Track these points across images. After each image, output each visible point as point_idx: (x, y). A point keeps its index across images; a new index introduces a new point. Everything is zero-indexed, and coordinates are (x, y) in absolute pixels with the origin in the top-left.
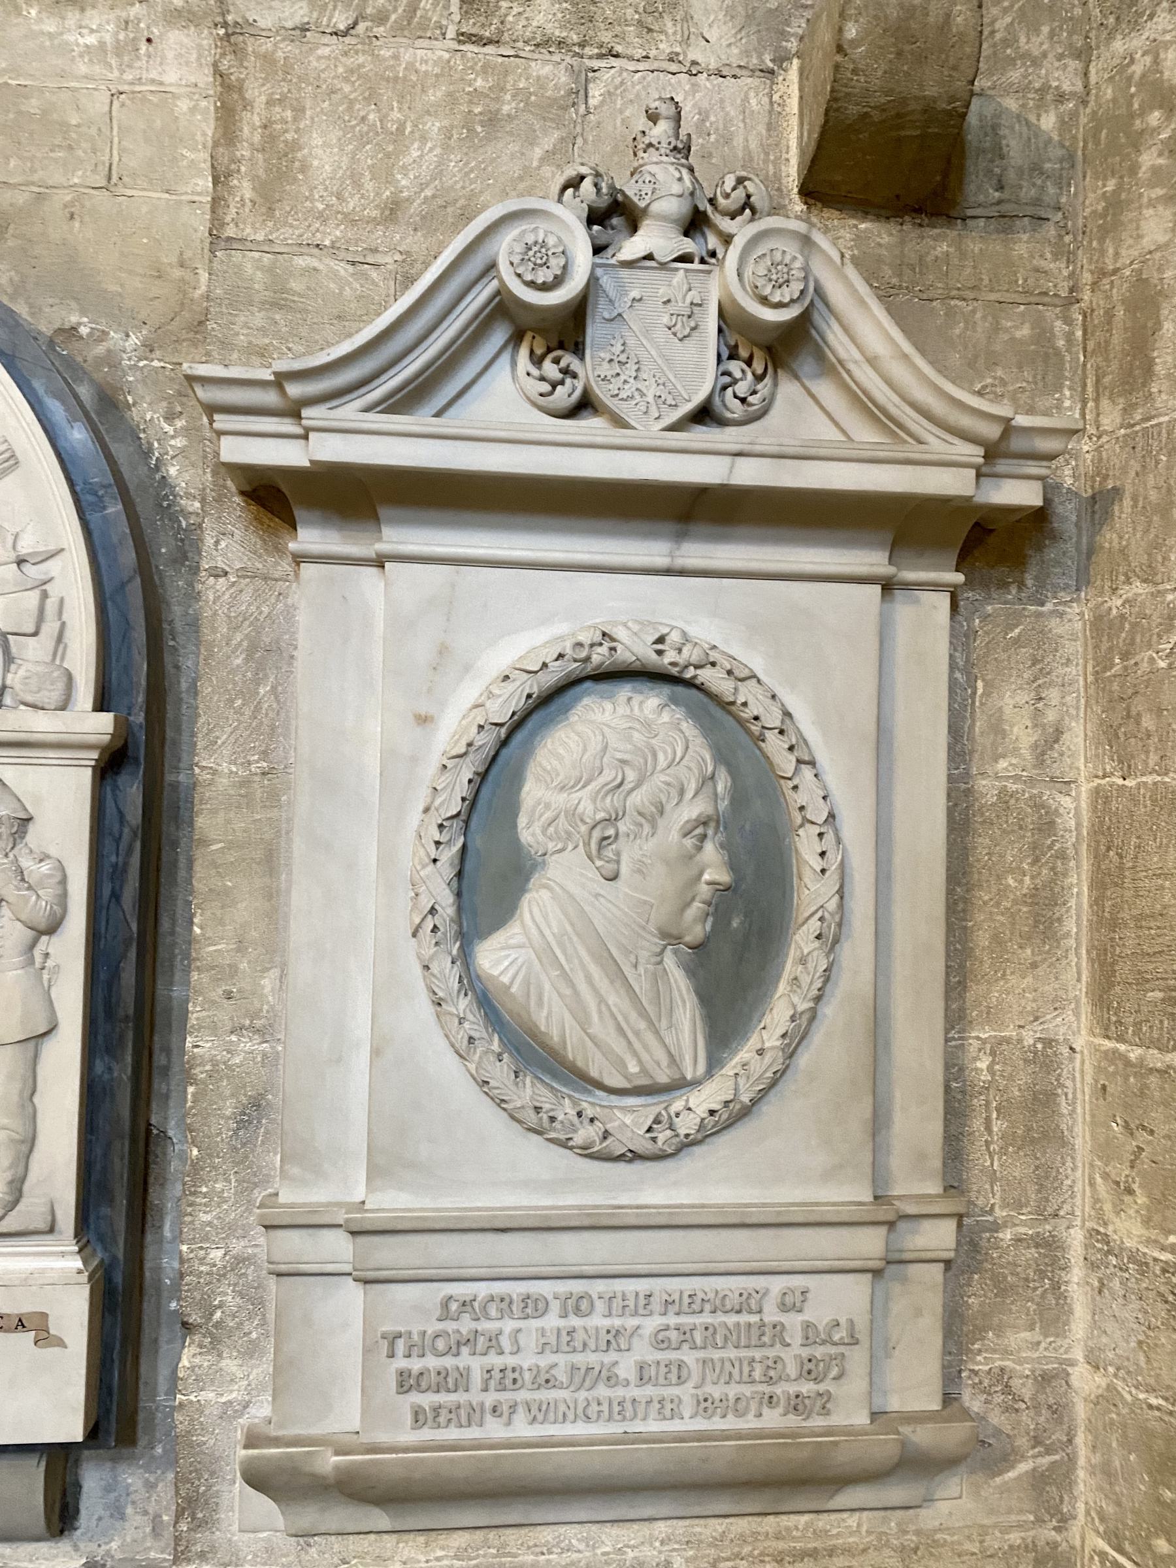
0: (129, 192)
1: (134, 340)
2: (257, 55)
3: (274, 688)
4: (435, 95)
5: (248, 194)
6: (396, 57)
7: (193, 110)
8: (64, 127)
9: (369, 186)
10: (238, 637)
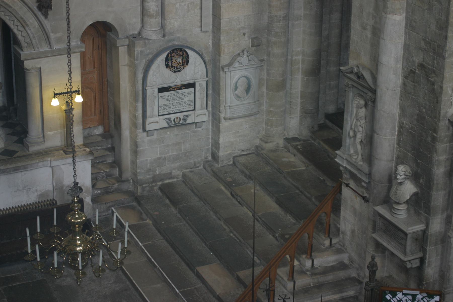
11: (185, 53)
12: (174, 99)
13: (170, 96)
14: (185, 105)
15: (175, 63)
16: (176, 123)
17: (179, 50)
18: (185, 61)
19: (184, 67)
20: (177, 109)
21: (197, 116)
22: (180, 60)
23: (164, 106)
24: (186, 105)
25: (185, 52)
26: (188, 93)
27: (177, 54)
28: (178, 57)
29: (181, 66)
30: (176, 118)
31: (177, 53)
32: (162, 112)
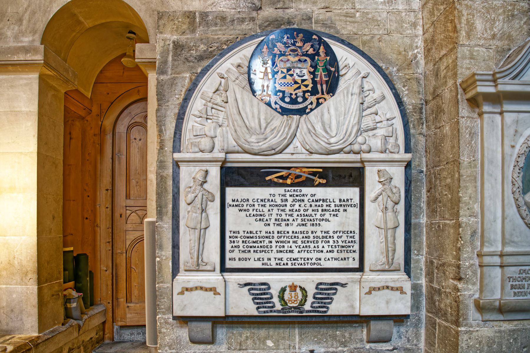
0: (392, 35)
1: (395, 69)
2: (464, 5)
3: (475, 142)
4: (501, 11)
5: (464, 34)
6: (492, 3)
7: (406, 15)
8: (377, 21)
9: (489, 31)
10: (467, 131)
11: (322, 50)
12: (284, 217)
13: (270, 206)
14: (326, 245)
15: (283, 81)
16: (291, 307)
17: (301, 35)
18: (321, 77)
19: (318, 99)
20: (296, 255)
21: (369, 293)
22: (305, 71)
23: (248, 238)
24: (330, 249)
25: (322, 47)
26: (338, 203)
27: (293, 48)
28: (297, 59)
29: (307, 95)
30: (288, 289)
31: (294, 45)
32: (240, 259)
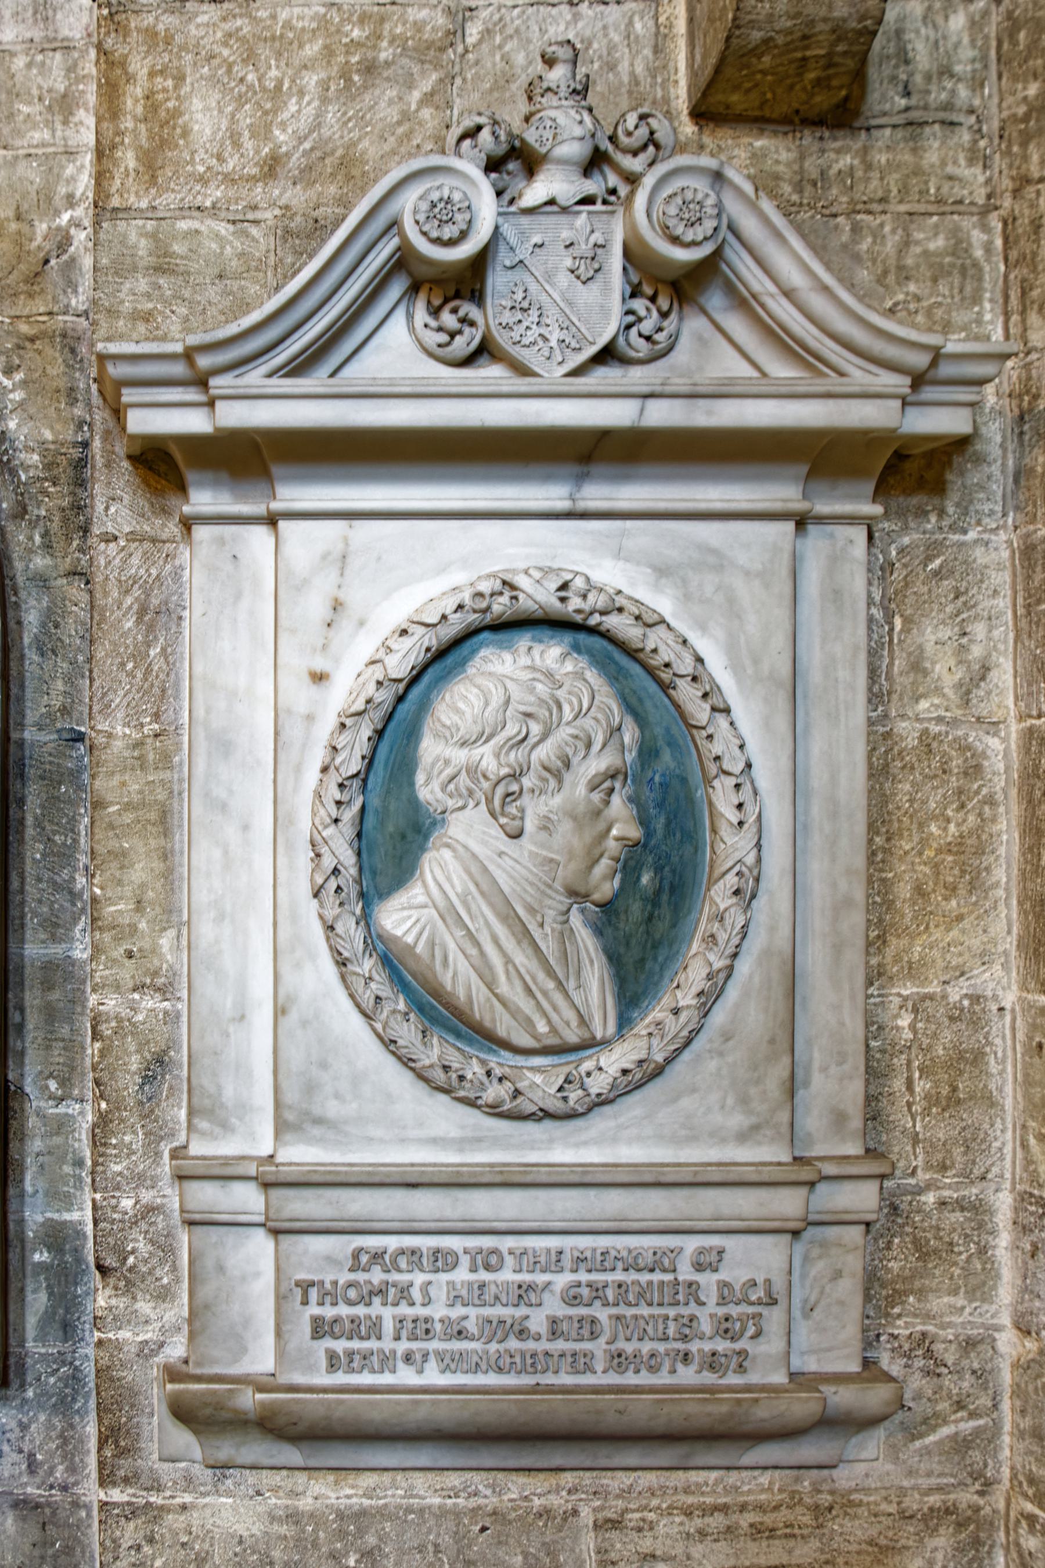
2: (138, 30)
3: (164, 650)
4: (312, 49)
5: (132, 164)
6: (274, 17)
9: (248, 144)
10: (129, 600)
